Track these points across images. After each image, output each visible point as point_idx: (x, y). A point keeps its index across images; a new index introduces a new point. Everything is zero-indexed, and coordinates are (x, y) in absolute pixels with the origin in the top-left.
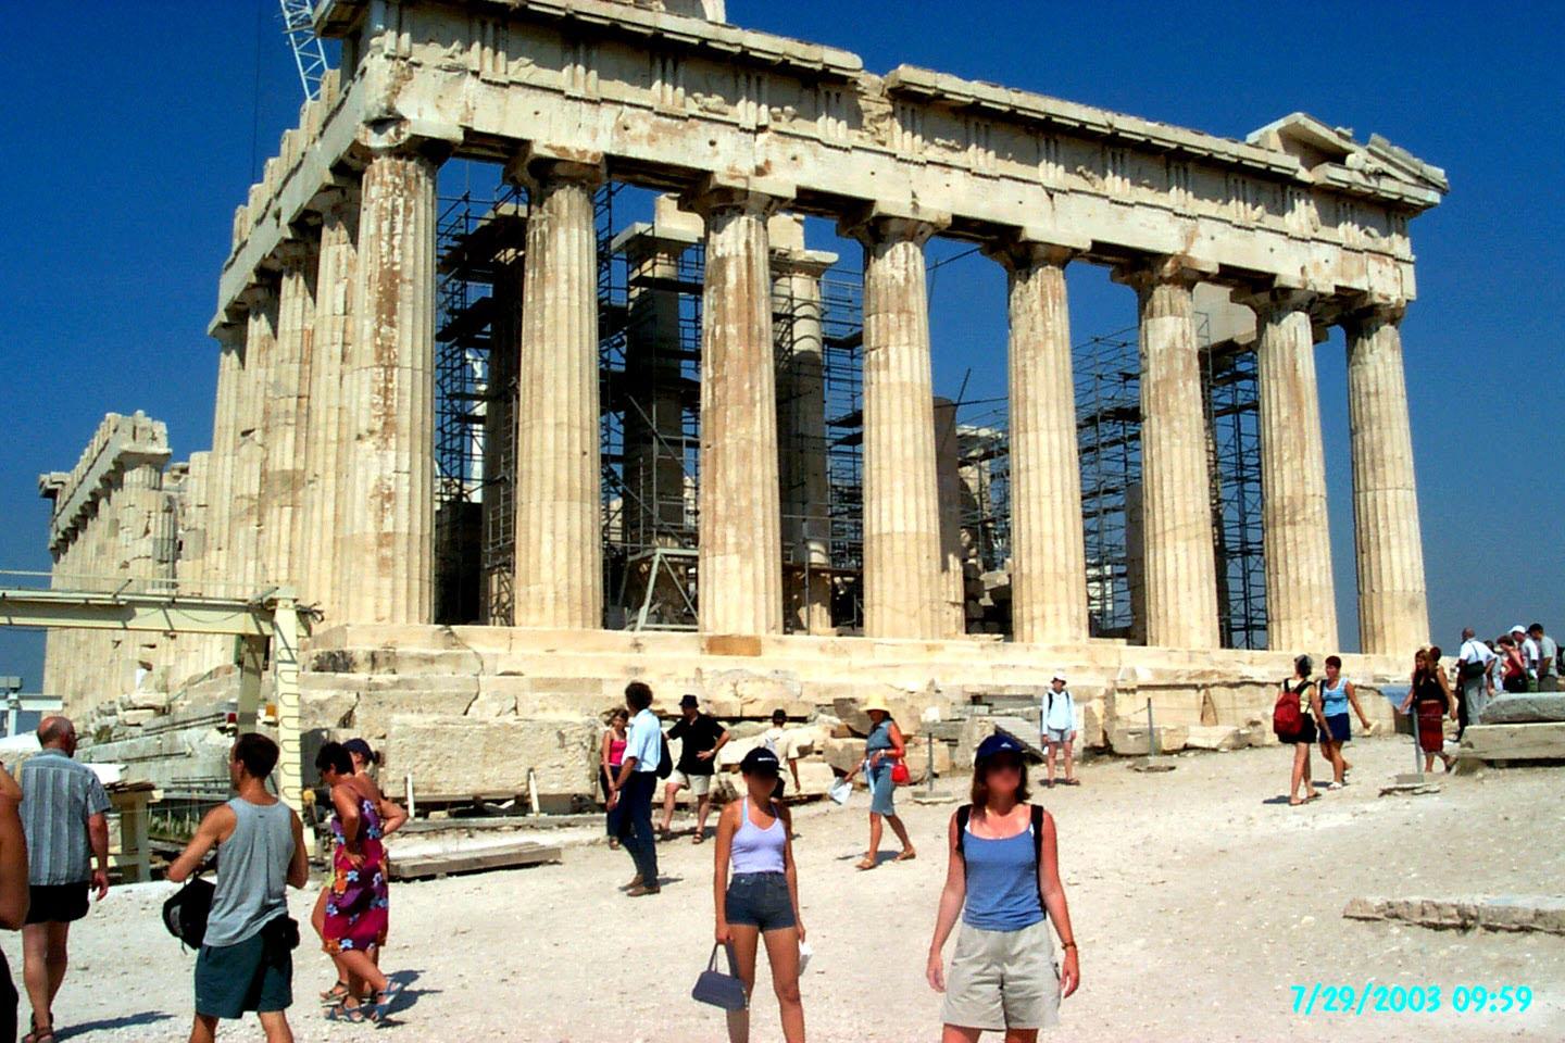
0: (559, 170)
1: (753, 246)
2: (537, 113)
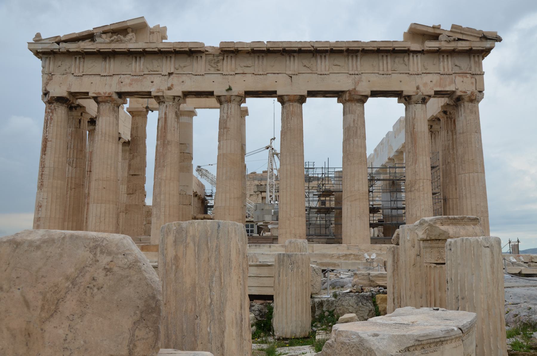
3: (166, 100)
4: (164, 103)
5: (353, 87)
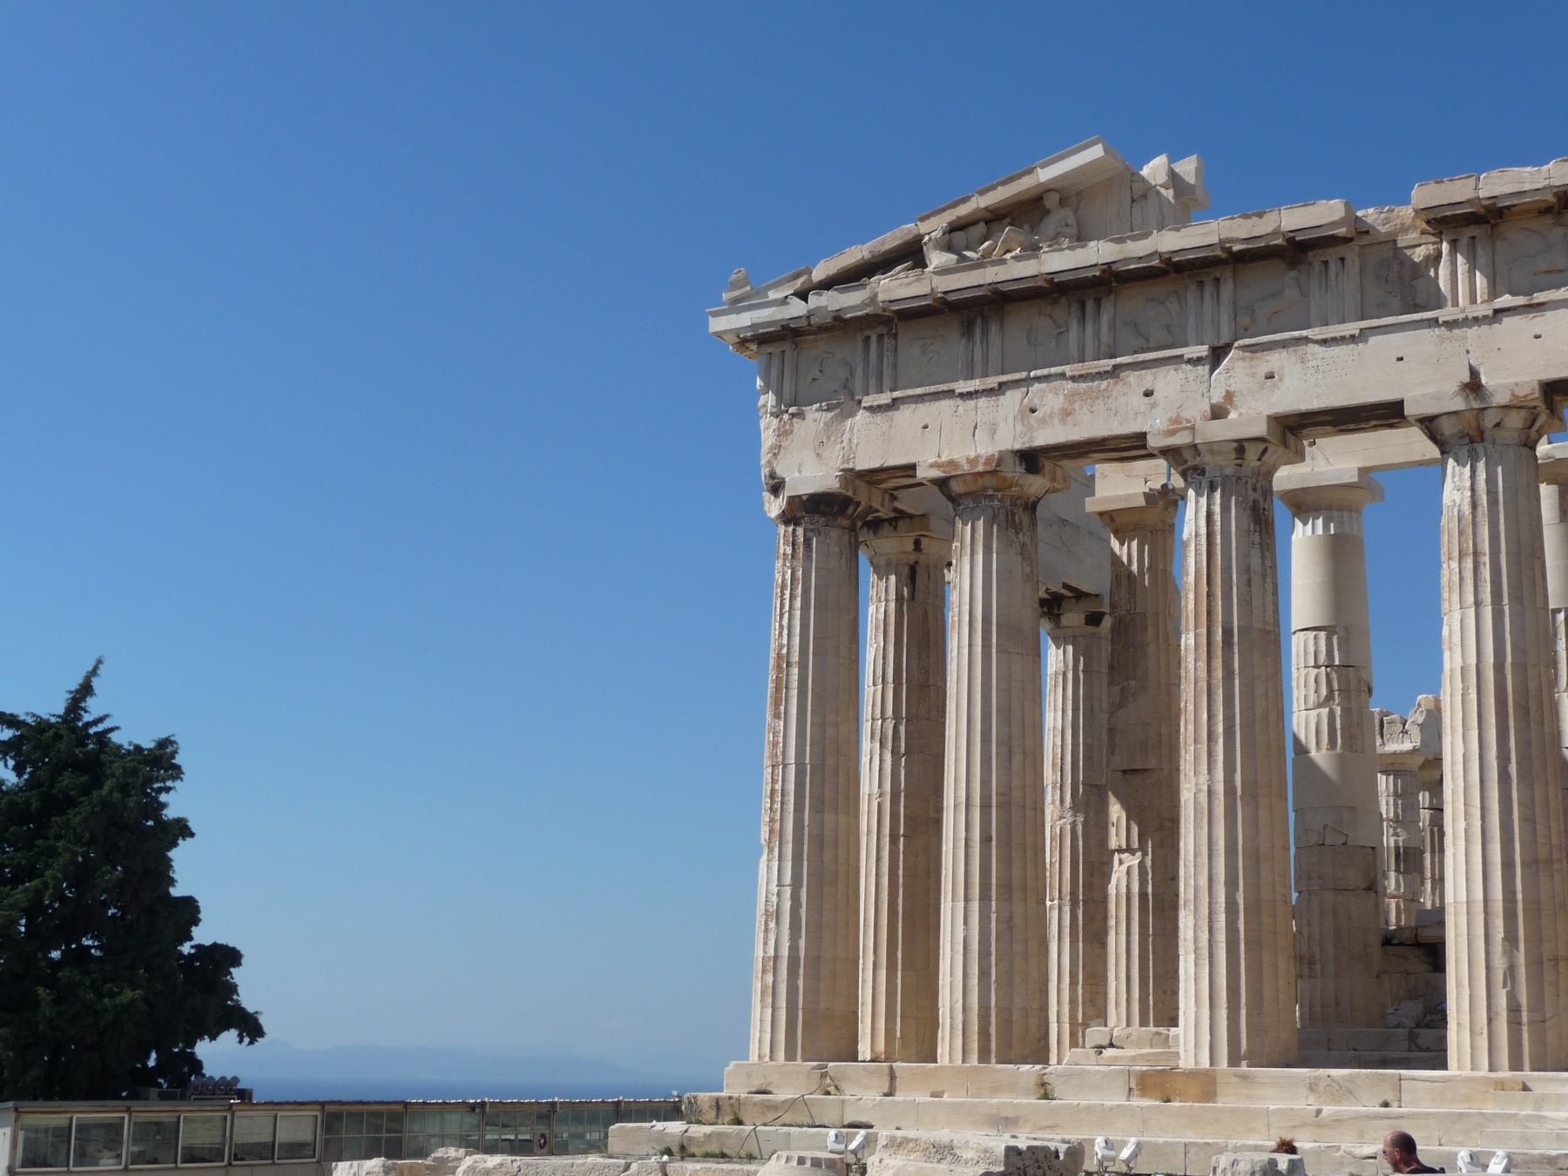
0: (957, 487)
1: (1217, 517)
2: (926, 427)
3: (1208, 458)
4: (1203, 473)
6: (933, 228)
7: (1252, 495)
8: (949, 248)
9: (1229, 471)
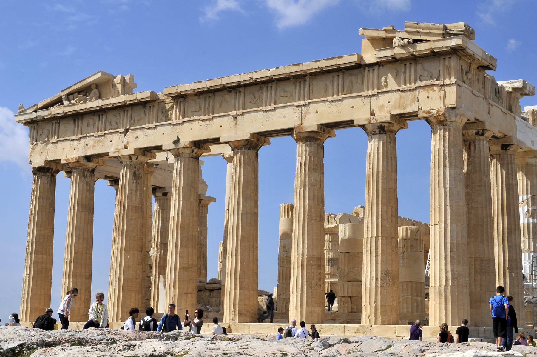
5: (299, 123)
6: (64, 94)
7: (134, 170)
8: (68, 100)
9: (128, 163)
